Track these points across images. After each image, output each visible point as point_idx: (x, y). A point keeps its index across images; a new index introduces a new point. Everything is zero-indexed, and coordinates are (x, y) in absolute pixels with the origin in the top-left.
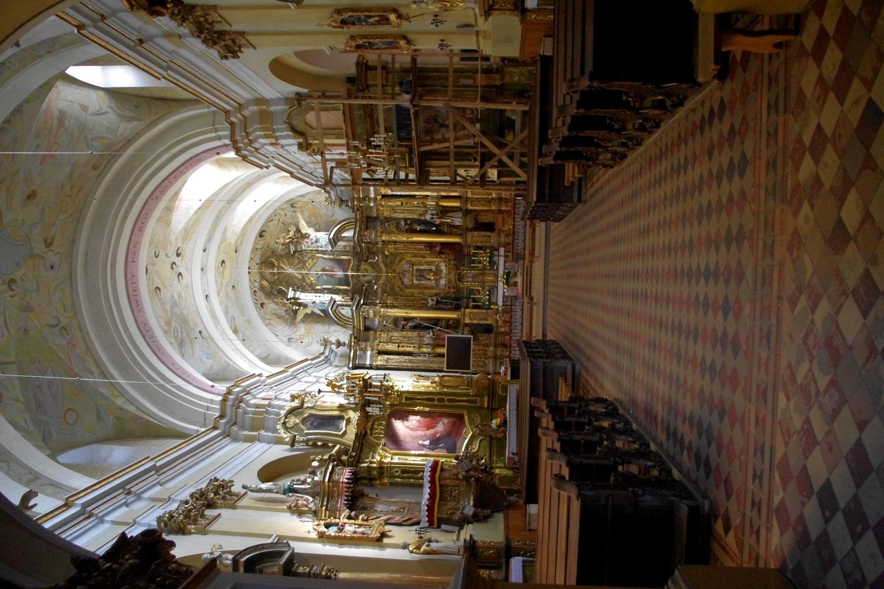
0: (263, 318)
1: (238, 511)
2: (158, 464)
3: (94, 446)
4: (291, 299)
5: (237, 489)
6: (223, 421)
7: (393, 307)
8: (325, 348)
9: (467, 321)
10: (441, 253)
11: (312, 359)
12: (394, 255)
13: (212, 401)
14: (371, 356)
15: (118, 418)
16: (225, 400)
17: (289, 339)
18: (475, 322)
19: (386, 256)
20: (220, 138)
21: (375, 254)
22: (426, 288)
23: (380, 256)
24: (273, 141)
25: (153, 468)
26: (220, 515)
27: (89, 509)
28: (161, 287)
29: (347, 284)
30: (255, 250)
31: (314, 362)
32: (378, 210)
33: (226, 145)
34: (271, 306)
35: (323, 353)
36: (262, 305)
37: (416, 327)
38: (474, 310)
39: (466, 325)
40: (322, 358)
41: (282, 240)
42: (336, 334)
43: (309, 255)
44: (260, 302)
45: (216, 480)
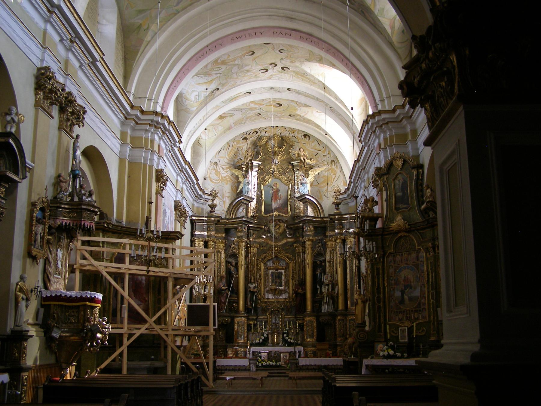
0: (234, 140)
1: (56, 132)
2: (98, 64)
3: (116, 9)
5: (77, 130)
6: (138, 113)
7: (247, 253)
8: (208, 194)
9: (236, 320)
10: (296, 293)
11: (198, 184)
12: (294, 253)
13: (156, 103)
15: (140, 26)
16: (156, 113)
17: (216, 163)
18: (236, 327)
20: (382, 101)
23: (292, 240)
24: (382, 146)
25: (95, 60)
26: (53, 118)
27: (56, 11)
28: (254, 55)
29: (266, 212)
30: (293, 131)
31: (196, 186)
32: (331, 236)
33: (376, 106)
34: (245, 146)
35: (204, 193)
36: (246, 139)
37: (229, 274)
38: (246, 325)
39: (233, 319)
40: (200, 193)
41: (302, 153)
42: (222, 203)
44: (248, 137)
45: (84, 112)
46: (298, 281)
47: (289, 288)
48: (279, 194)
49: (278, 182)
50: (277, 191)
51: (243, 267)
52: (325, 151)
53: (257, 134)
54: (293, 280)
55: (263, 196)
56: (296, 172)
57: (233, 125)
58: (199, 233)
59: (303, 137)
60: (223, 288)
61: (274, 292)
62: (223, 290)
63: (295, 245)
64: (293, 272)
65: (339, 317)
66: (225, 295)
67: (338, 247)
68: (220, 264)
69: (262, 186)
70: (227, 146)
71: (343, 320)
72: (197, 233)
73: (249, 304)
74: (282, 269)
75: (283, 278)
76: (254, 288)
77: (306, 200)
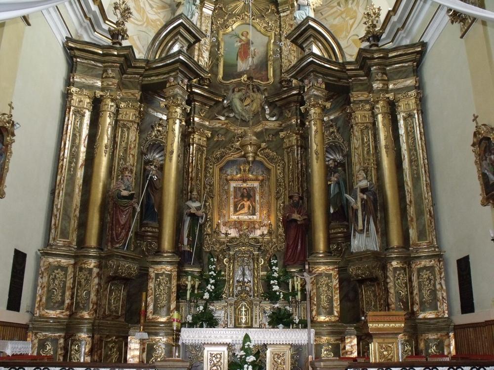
10: (288, 223)
12: (279, 147)
14: (91, 87)
19: (277, 133)
21: (280, 116)
29: (226, 76)
48: (252, 48)
49: (250, 30)
50: (248, 44)
55: (222, 51)
60: (125, 193)
63: (282, 134)
66: (131, 210)
67: (380, 117)
69: (221, 33)
73: (186, 242)
76: (198, 209)
77: (310, 32)
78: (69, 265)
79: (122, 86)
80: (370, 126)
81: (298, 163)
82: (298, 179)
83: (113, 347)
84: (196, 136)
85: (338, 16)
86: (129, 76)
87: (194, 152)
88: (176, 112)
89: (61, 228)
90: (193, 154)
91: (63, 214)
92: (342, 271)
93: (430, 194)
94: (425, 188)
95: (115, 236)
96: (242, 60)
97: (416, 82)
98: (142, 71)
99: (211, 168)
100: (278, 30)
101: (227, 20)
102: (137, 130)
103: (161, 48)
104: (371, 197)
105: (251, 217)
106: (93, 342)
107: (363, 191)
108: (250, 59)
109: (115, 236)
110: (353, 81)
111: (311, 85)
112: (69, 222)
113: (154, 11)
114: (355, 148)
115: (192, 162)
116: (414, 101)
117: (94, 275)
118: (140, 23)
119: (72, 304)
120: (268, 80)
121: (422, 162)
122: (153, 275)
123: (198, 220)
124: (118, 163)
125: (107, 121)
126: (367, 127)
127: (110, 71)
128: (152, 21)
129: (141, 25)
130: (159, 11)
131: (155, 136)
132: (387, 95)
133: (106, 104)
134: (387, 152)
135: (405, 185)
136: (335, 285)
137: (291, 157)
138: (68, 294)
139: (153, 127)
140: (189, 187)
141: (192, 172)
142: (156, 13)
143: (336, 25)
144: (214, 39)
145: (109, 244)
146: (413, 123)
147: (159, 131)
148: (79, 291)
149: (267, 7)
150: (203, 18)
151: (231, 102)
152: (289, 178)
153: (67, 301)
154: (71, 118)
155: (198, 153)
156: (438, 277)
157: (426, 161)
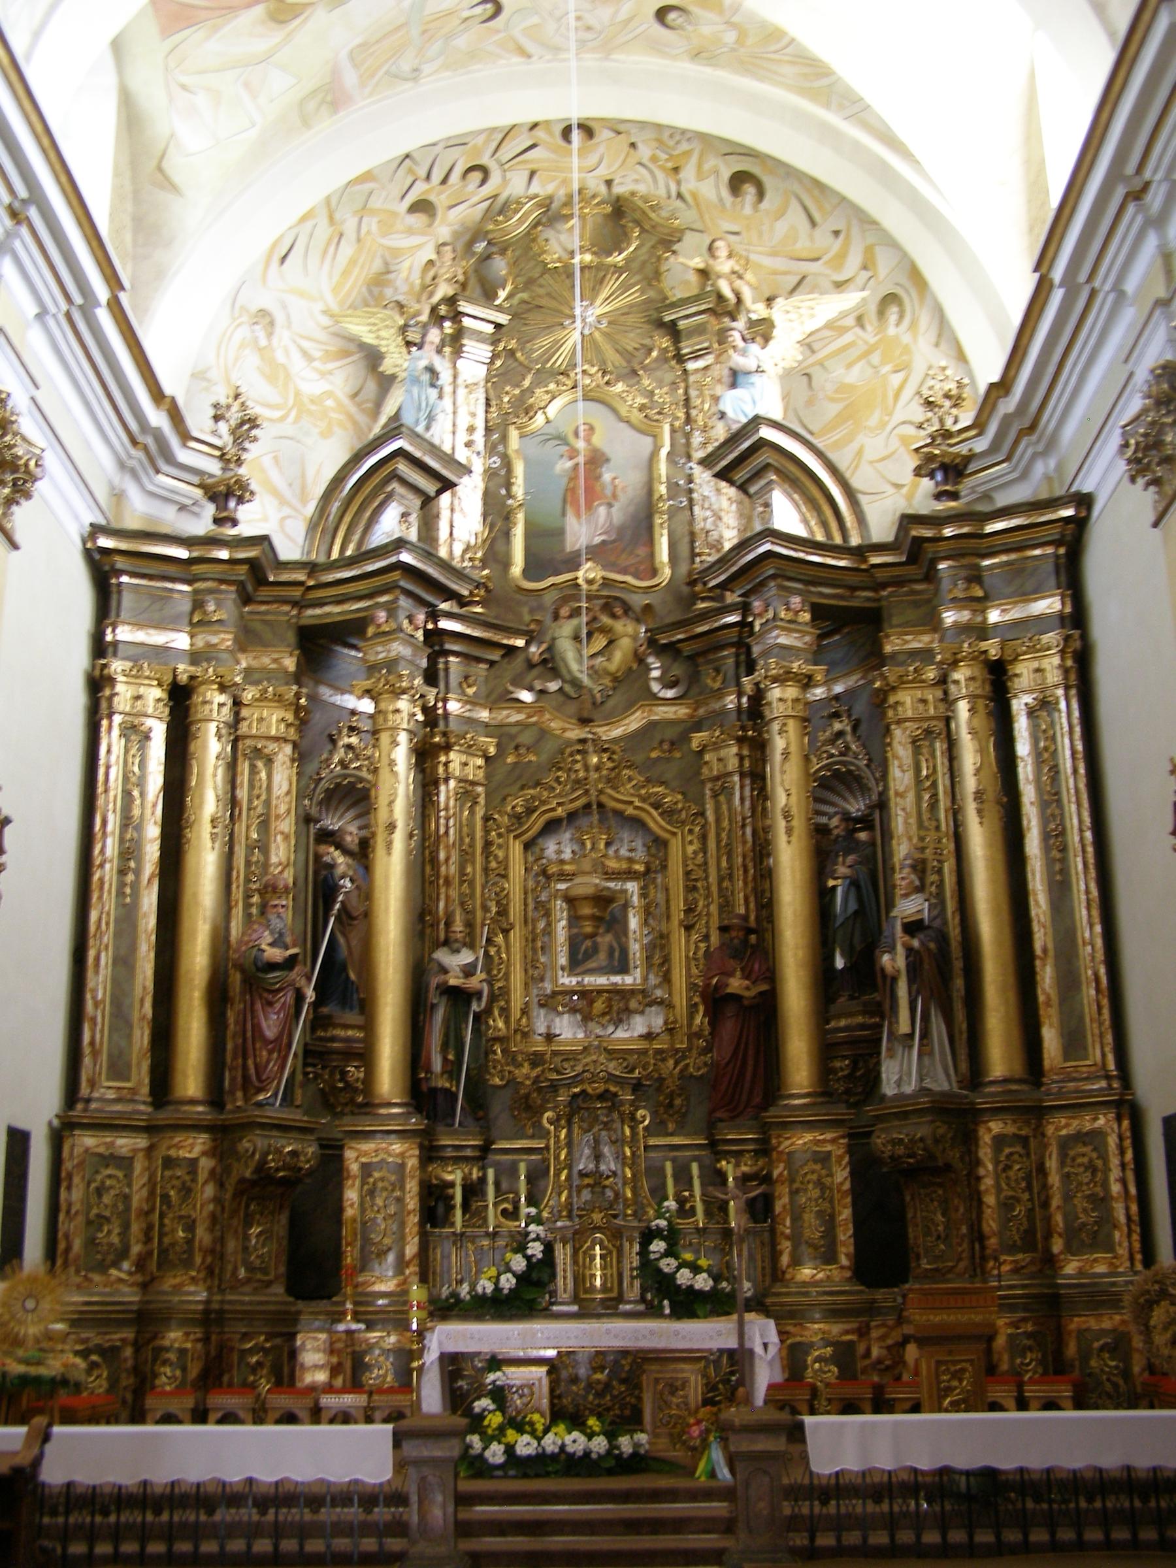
4: (457, 316)
9: (354, 1157)
10: (716, 1002)
12: (692, 778)
14: (162, 652)
18: (351, 1195)
19: (685, 738)
22: (538, 943)
23: (682, 712)
29: (534, 568)
36: (422, 207)
37: (324, 888)
38: (412, 1186)
39: (332, 1154)
40: (157, 418)
41: (724, 266)
43: (662, 395)
44: (440, 199)
46: (723, 929)
47: (667, 979)
48: (607, 477)
49: (599, 416)
50: (597, 460)
51: (399, 838)
52: (842, 256)
53: (487, 190)
54: (688, 928)
55: (519, 490)
56: (691, 366)
57: (350, 78)
58: (140, 636)
59: (725, 193)
60: (275, 954)
61: (584, 1004)
62: (272, 966)
64: (691, 889)
65: (996, 1127)
66: (289, 997)
67: (963, 707)
68: (265, 825)
69: (513, 433)
70: (324, 231)
71: (1024, 1141)
72: (124, 633)
73: (437, 1064)
74: (630, 875)
75: (634, 923)
76: (469, 971)
77: (764, 457)
78: (135, 1151)
79: (247, 638)
80: (939, 726)
81: (744, 826)
82: (746, 871)
83: (259, 1364)
84: (455, 758)
85: (859, 359)
86: (263, 608)
87: (452, 803)
88: (397, 711)
89: (110, 1055)
90: (447, 809)
91: (111, 1015)
92: (858, 1140)
93: (1098, 929)
94: (1084, 912)
95: (252, 1071)
96: (578, 515)
97: (1063, 604)
98: (297, 593)
99: (500, 846)
100: (681, 414)
101: (530, 391)
102: (293, 760)
103: (347, 519)
104: (932, 945)
105: (617, 979)
106: (207, 1354)
107: (913, 928)
108: (602, 510)
109: (252, 1071)
110: (891, 595)
111: (770, 615)
112: (129, 1036)
113: (316, 369)
114: (897, 794)
115: (447, 833)
116: (1056, 660)
117: (202, 1175)
118: (277, 414)
119: (150, 1253)
120: (654, 572)
121: (1077, 839)
122: (354, 1168)
123: (469, 1005)
124: (248, 863)
125: (211, 747)
126: (928, 732)
127: (211, 607)
128: (312, 401)
129: (283, 419)
130: (331, 366)
131: (342, 762)
132: (984, 645)
133: (205, 702)
134: (979, 812)
135: (1032, 903)
136: (842, 1184)
137: (724, 807)
138: (136, 1228)
139: (333, 740)
140: (442, 905)
141: (447, 860)
142: (323, 374)
143: (852, 387)
144: (496, 462)
145: (239, 1094)
146: (1052, 724)
147: (349, 747)
148: (166, 1221)
149: (647, 341)
150: (462, 392)
151: (550, 649)
152: (719, 868)
153: (136, 1249)
154: (115, 749)
155: (462, 807)
156: (1115, 1161)
157: (1088, 835)
